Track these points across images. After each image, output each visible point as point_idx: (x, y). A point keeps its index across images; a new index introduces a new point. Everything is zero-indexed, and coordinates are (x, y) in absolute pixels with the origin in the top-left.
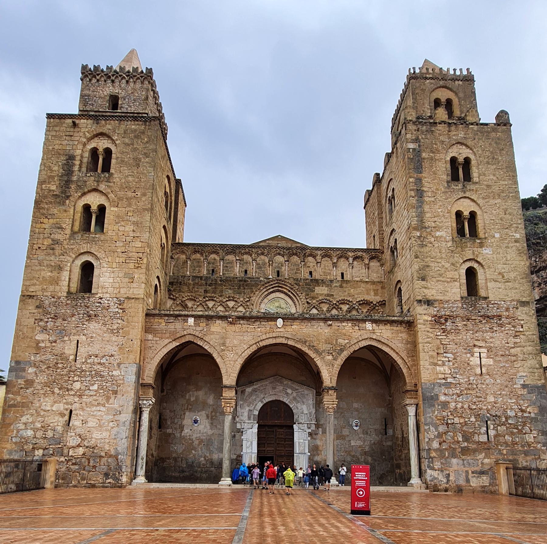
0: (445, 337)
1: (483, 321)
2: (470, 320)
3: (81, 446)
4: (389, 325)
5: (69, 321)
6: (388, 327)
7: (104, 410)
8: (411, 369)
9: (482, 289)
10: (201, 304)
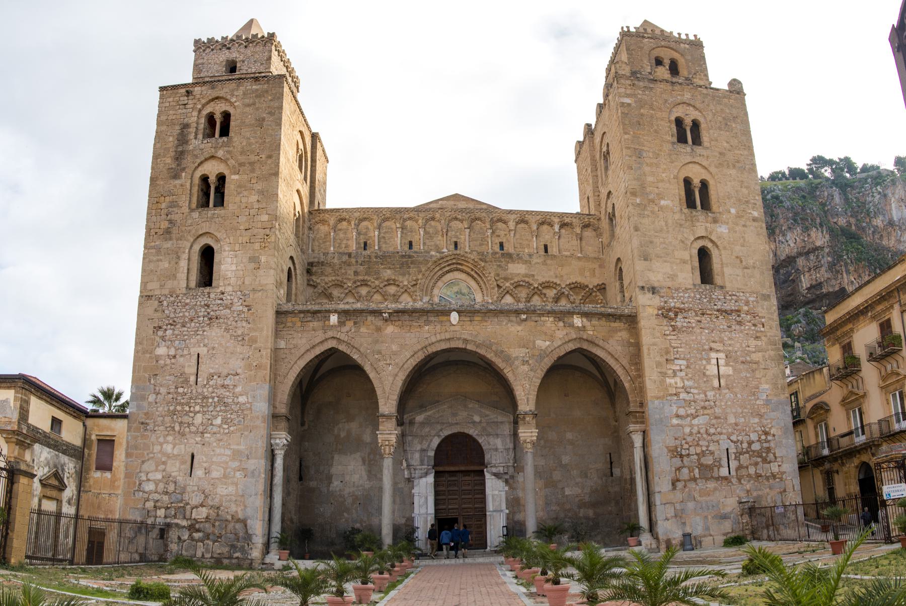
0: (675, 337)
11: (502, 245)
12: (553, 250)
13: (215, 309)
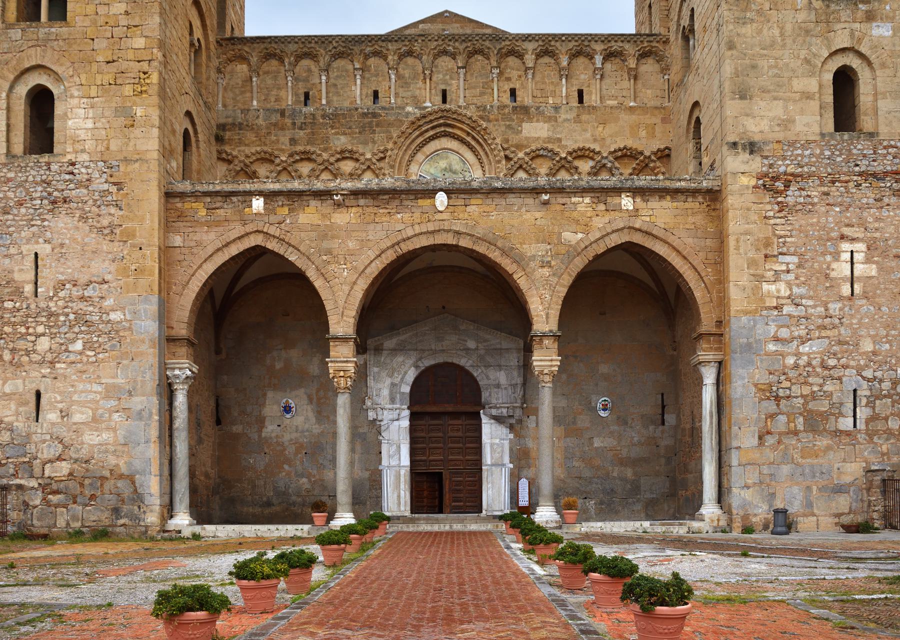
0: (783, 221)
1: (864, 185)
2: (837, 184)
3: (64, 460)
4: (668, 198)
5: (15, 215)
6: (667, 203)
7: (100, 390)
8: (711, 291)
9: (866, 115)
10: (285, 169)
11: (513, 92)
12: (592, 98)
13: (60, 187)
